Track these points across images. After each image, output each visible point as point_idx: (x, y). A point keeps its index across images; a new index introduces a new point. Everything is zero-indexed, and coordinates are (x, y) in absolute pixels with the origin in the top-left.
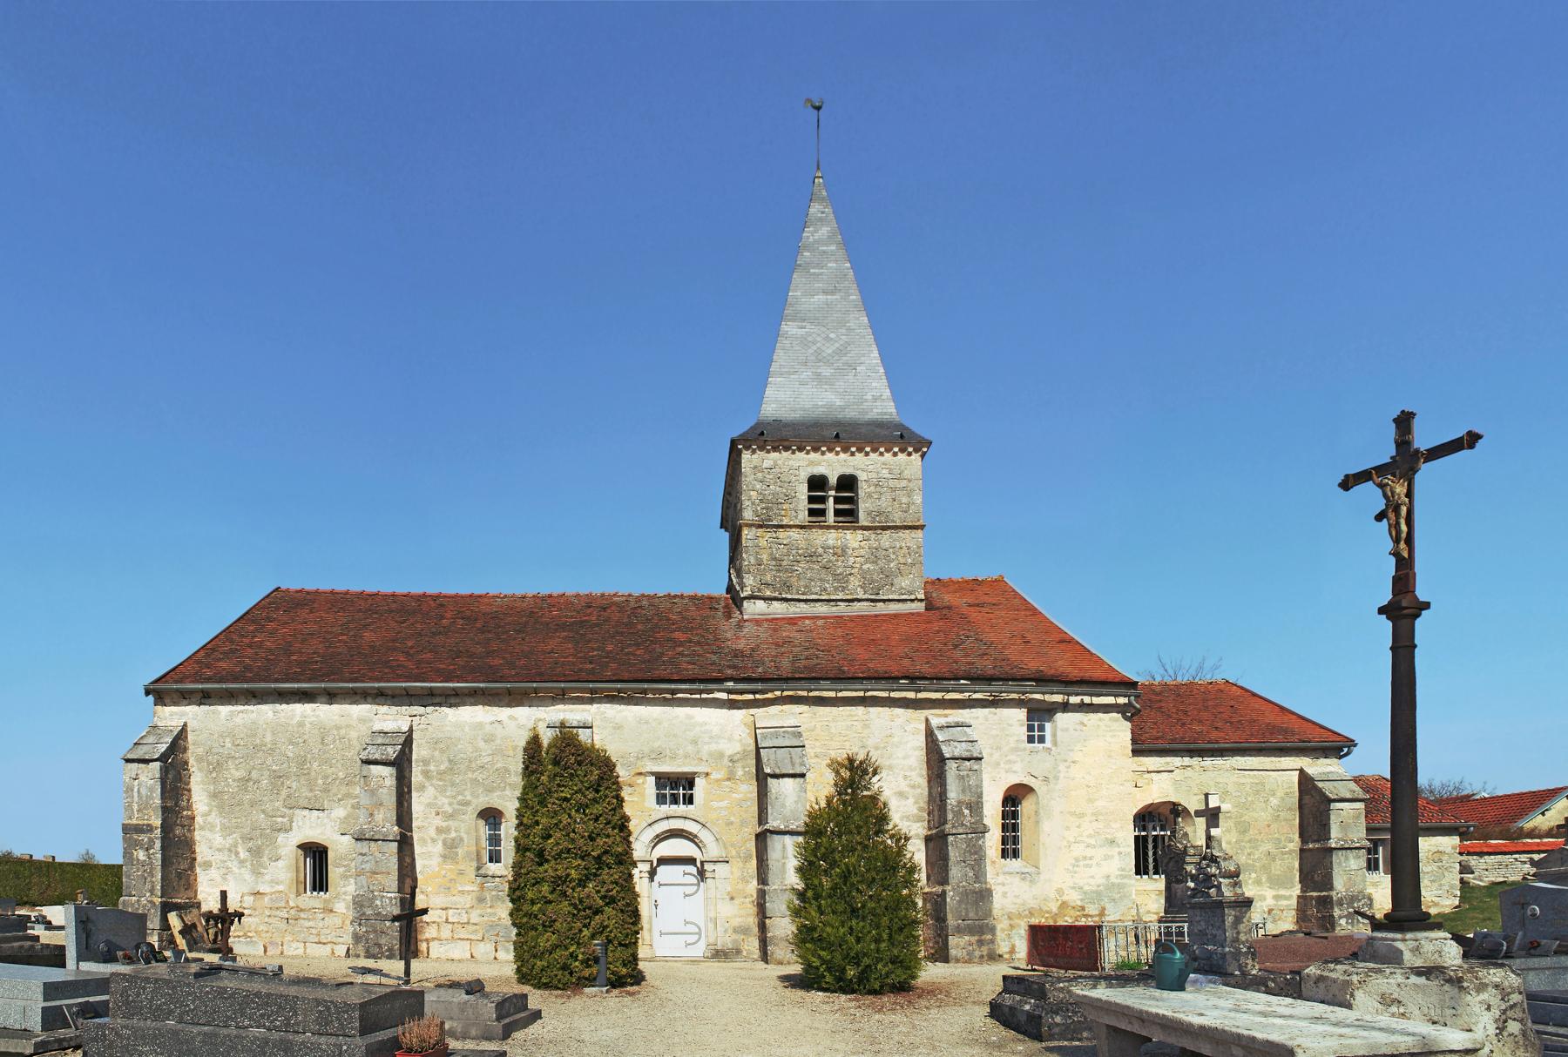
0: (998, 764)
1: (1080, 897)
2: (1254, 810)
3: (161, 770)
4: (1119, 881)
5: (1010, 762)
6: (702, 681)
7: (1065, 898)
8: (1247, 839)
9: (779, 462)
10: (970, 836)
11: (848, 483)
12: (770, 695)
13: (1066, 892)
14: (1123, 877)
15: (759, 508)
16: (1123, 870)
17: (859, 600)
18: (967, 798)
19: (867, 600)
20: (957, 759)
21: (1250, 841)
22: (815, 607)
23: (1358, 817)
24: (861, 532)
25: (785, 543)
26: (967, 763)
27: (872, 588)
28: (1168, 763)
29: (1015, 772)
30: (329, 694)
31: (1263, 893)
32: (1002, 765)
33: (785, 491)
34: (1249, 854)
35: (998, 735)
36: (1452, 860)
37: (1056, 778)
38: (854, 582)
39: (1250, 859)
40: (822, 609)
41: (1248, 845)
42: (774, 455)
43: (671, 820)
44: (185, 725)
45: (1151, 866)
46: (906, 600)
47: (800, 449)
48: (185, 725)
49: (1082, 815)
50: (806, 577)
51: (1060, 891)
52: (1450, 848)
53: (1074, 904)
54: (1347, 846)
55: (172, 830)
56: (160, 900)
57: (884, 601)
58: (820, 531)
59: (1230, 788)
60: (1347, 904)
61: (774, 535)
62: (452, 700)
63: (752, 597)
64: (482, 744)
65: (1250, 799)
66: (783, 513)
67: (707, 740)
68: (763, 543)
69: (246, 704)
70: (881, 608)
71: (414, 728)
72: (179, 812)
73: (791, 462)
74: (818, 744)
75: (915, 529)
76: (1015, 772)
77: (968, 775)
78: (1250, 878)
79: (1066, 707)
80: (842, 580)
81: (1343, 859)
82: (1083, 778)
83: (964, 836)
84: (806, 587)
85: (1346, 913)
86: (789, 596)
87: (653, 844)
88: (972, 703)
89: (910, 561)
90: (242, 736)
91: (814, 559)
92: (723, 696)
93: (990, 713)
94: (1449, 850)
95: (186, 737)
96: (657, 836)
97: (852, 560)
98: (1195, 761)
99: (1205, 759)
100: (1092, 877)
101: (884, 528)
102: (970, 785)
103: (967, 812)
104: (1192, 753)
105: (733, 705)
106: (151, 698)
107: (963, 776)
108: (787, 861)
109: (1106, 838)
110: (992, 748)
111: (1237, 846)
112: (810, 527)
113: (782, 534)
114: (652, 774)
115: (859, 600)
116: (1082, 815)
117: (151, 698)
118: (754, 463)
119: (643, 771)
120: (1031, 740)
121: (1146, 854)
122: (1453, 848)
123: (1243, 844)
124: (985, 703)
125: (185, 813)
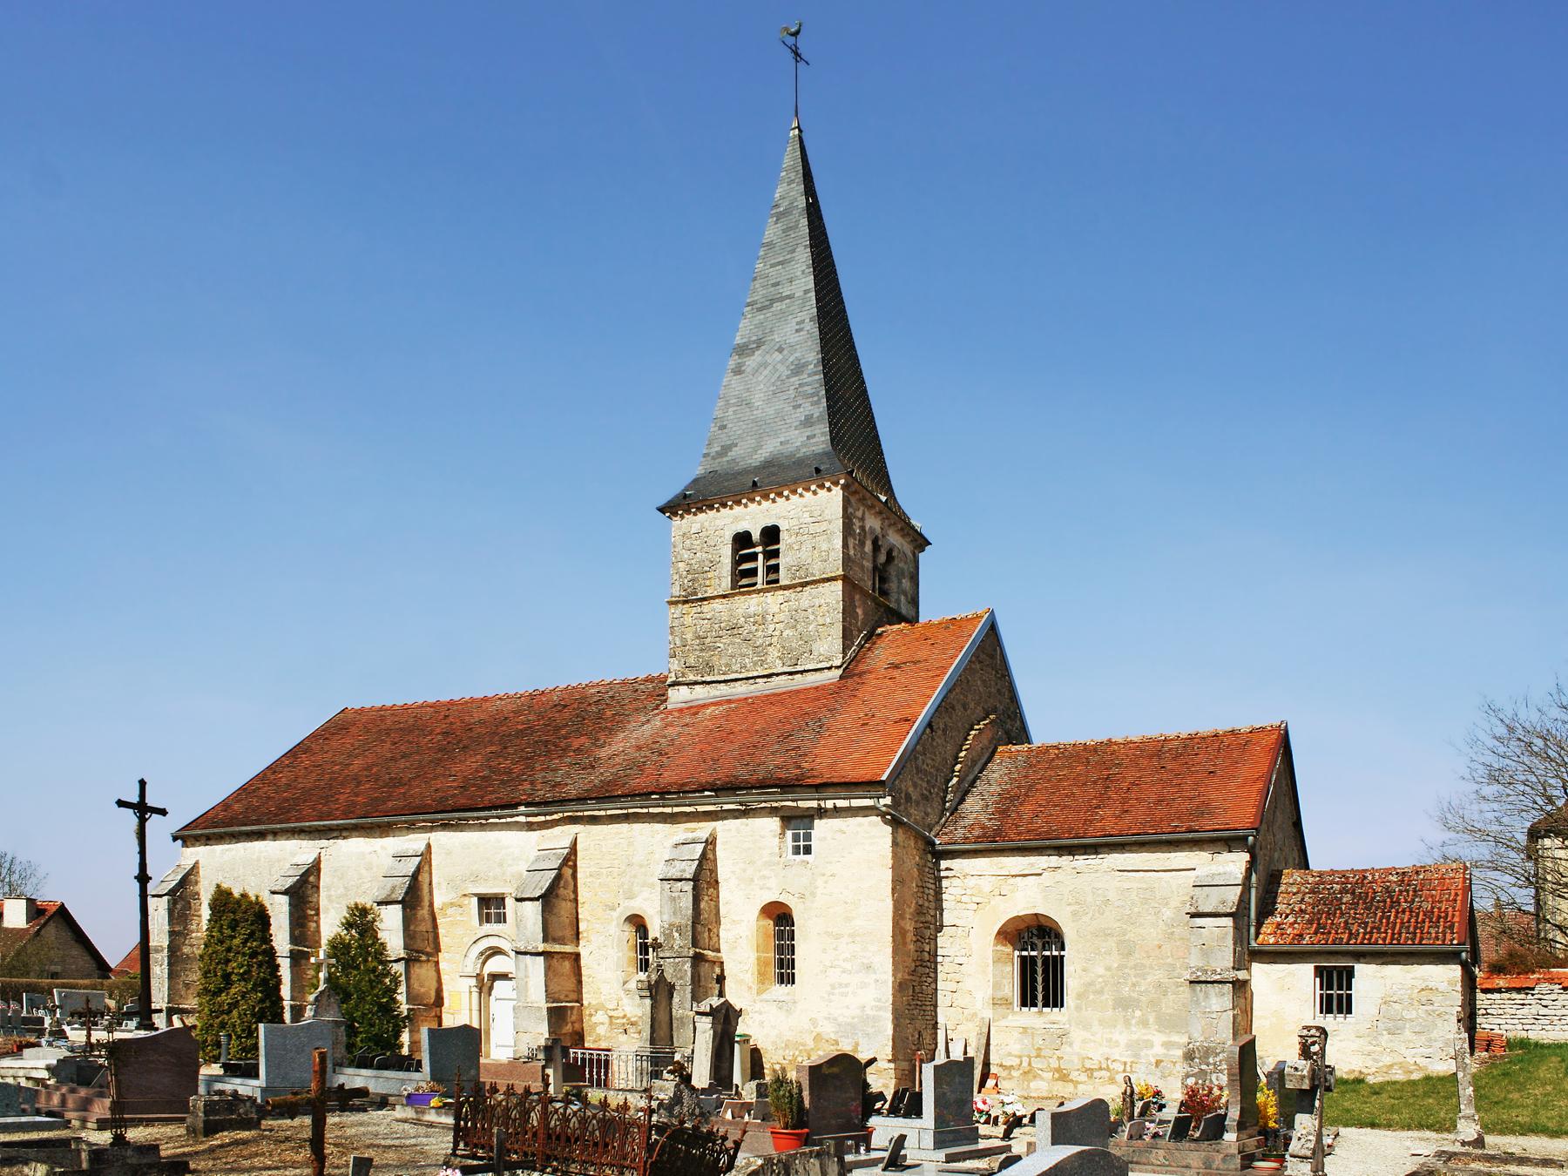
0: (752, 880)
1: (833, 1030)
2: (1141, 925)
3: (168, 902)
4: (875, 1013)
5: (764, 877)
6: (503, 807)
7: (819, 1030)
8: (1131, 964)
9: (706, 524)
10: (677, 960)
11: (771, 534)
12: (555, 817)
13: (821, 1023)
14: (880, 1009)
15: (686, 581)
16: (879, 1000)
17: (777, 675)
18: (677, 921)
19: (785, 673)
20: (669, 880)
21: (1135, 967)
22: (734, 687)
23: (1224, 938)
24: (781, 592)
25: (708, 617)
26: (679, 884)
27: (791, 658)
28: (1032, 865)
29: (769, 889)
30: (292, 831)
31: (1149, 1037)
32: (756, 881)
33: (710, 556)
34: (1134, 985)
35: (749, 849)
36: (1448, 1003)
37: (813, 894)
38: (774, 653)
39: (1134, 991)
40: (741, 689)
41: (1132, 972)
42: (701, 516)
43: (479, 943)
44: (197, 863)
45: (1040, 997)
46: (823, 669)
47: (724, 505)
48: (197, 863)
49: (838, 937)
50: (731, 656)
51: (814, 1022)
52: (1446, 984)
53: (826, 1037)
54: (1203, 979)
55: (180, 949)
56: (166, 1005)
57: (801, 672)
58: (742, 598)
59: (1112, 895)
60: (1200, 1058)
61: (699, 611)
62: (344, 834)
63: (674, 684)
64: (363, 872)
65: (1136, 910)
66: (708, 583)
67: (510, 862)
68: (688, 620)
69: (230, 843)
70: (800, 682)
71: (322, 859)
72: (187, 935)
73: (717, 522)
74: (592, 863)
75: (834, 580)
76: (769, 889)
77: (679, 897)
78: (1133, 1018)
79: (822, 813)
80: (760, 652)
81: (1201, 995)
82: (841, 893)
83: (672, 960)
84: (727, 665)
85: (1196, 1070)
86: (708, 679)
87: (481, 961)
88: (725, 814)
89: (828, 620)
90: (228, 869)
91: (735, 631)
92: (522, 819)
93: (742, 824)
94: (1443, 987)
95: (198, 872)
96: (482, 954)
97: (772, 627)
98: (1065, 861)
99: (1076, 857)
100: (848, 1007)
101: (804, 585)
102: (680, 907)
103: (676, 935)
104: (1061, 850)
105: (530, 827)
106: (179, 842)
107: (675, 897)
108: (528, 980)
109: (863, 963)
110: (745, 862)
111: (1120, 973)
112: (733, 595)
113: (706, 607)
114: (475, 895)
115: (777, 675)
116: (838, 937)
117: (179, 842)
118: (684, 530)
119: (467, 893)
120: (796, 851)
121: (1034, 980)
122: (1449, 983)
123: (1126, 971)
124: (737, 814)
125: (194, 935)
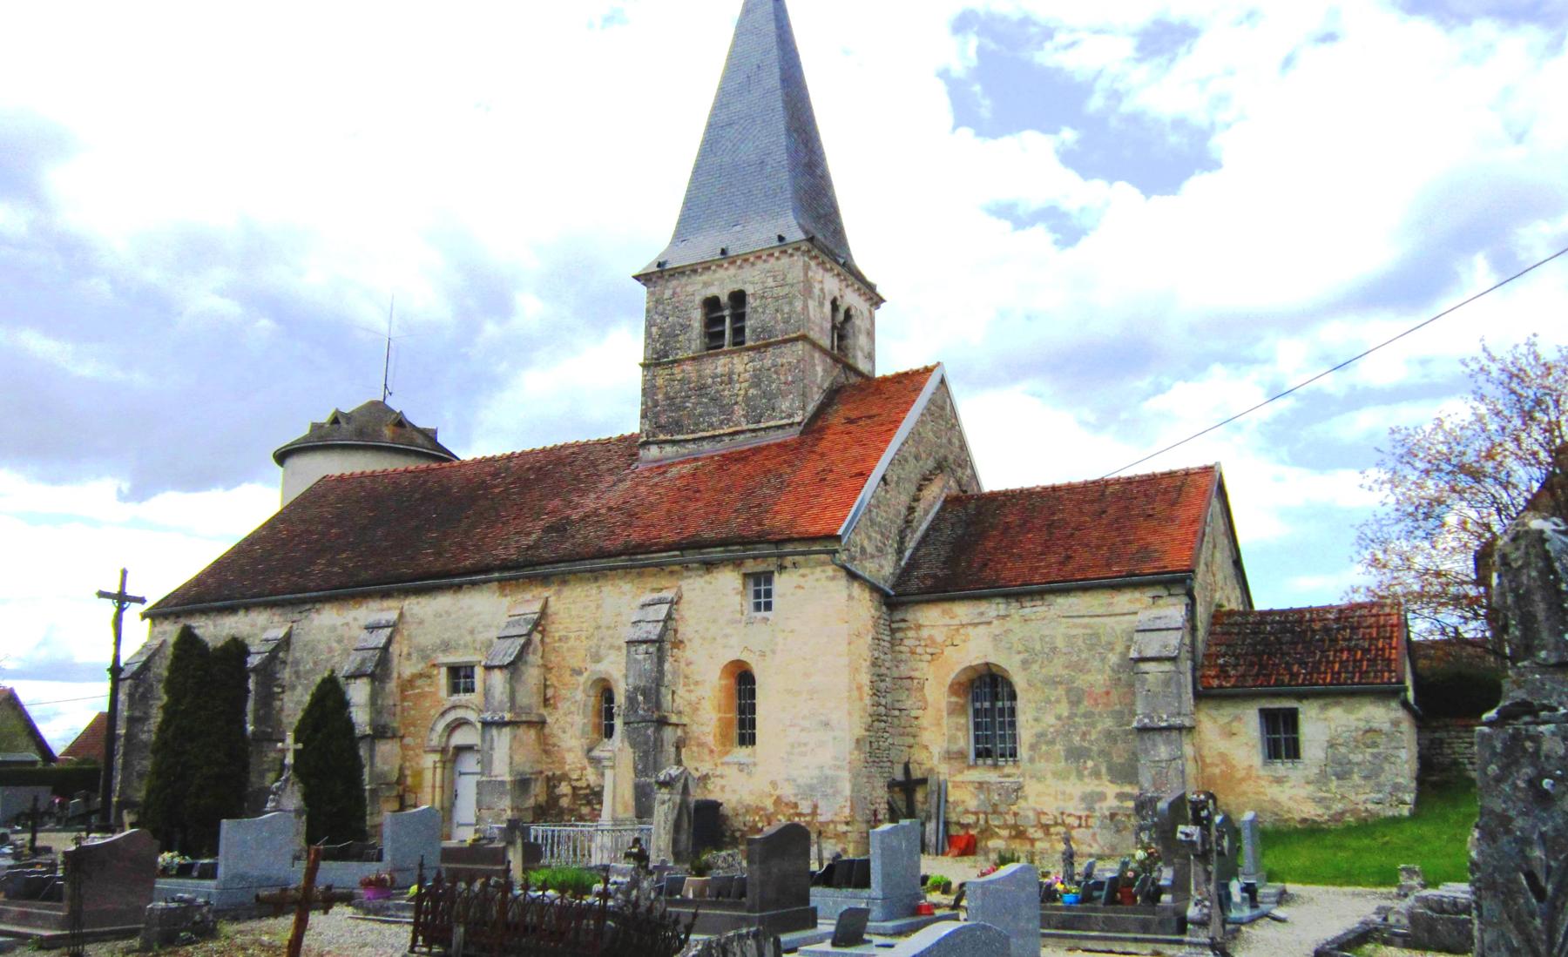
5: (726, 636)
7: (778, 792)
11: (738, 298)
14: (839, 768)
29: (732, 647)
51: (774, 784)
53: (786, 800)
91: (703, 391)
103: (640, 698)
120: (758, 607)
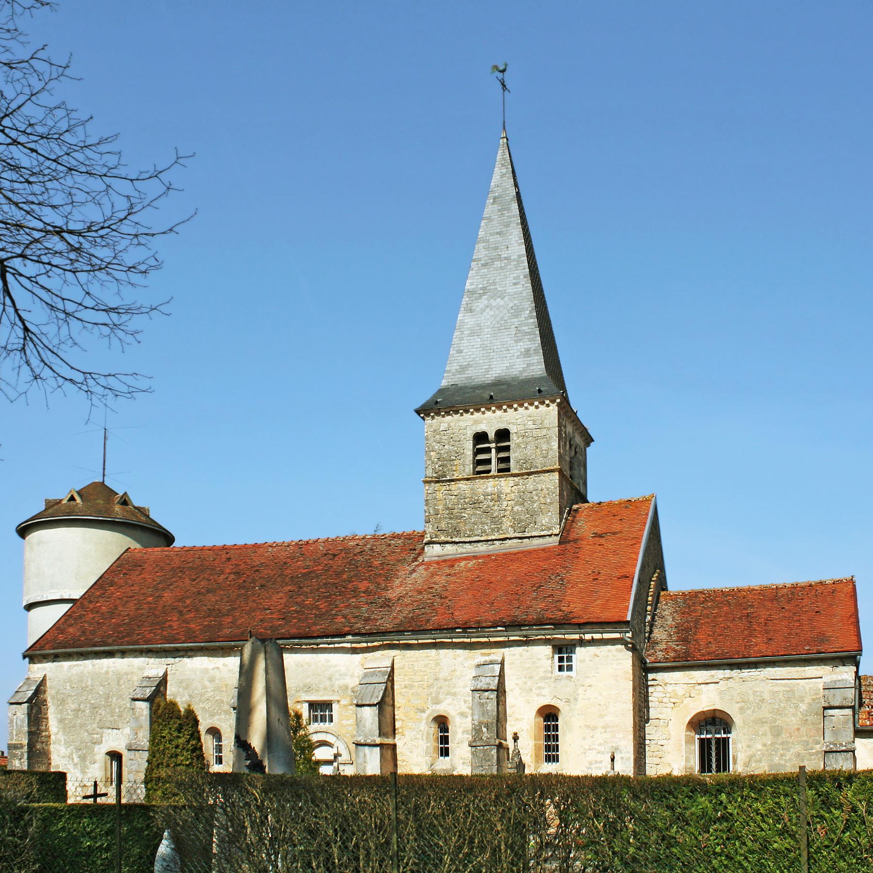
9: (452, 424)
11: (503, 435)
15: (437, 466)
17: (510, 539)
24: (512, 478)
27: (520, 527)
38: (507, 523)
40: (482, 548)
47: (467, 411)
57: (529, 538)
58: (482, 481)
61: (448, 489)
63: (430, 543)
66: (454, 468)
68: (440, 495)
70: (527, 544)
73: (461, 423)
80: (497, 521)
84: (471, 530)
86: (457, 540)
89: (548, 500)
113: (454, 486)
115: (510, 539)
